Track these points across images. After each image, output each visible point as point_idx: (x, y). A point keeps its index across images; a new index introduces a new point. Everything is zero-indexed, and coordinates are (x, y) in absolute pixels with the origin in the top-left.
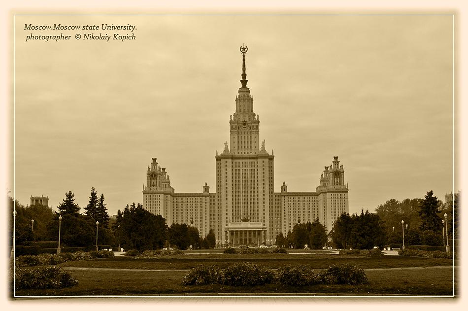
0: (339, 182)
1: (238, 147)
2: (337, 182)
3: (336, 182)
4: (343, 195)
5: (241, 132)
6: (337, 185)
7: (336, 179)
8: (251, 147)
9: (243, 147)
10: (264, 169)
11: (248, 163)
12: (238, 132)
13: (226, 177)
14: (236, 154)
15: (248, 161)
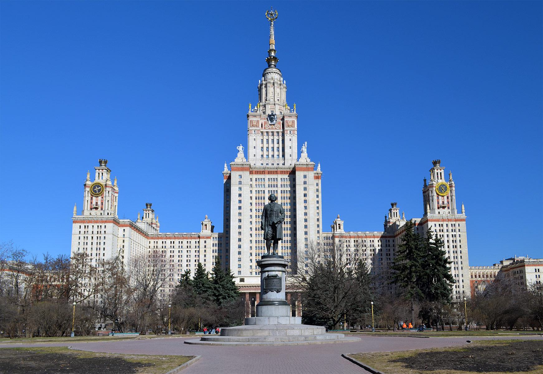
0: (446, 202)
1: (262, 156)
2: (443, 202)
3: (441, 203)
4: (457, 225)
5: (267, 132)
6: (444, 207)
7: (440, 197)
8: (283, 156)
9: (270, 156)
10: (305, 189)
11: (279, 180)
12: (262, 133)
13: (240, 201)
14: (258, 165)
15: (280, 177)
